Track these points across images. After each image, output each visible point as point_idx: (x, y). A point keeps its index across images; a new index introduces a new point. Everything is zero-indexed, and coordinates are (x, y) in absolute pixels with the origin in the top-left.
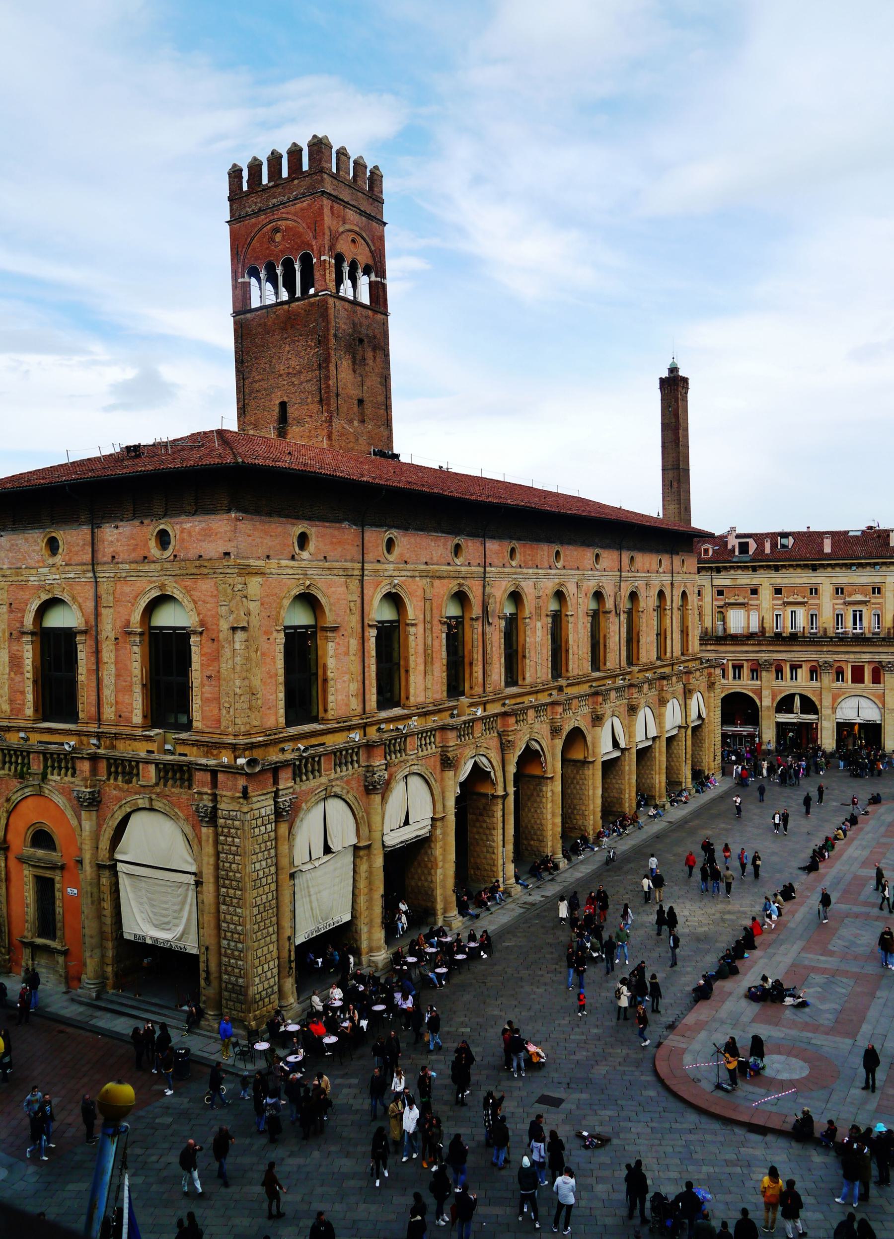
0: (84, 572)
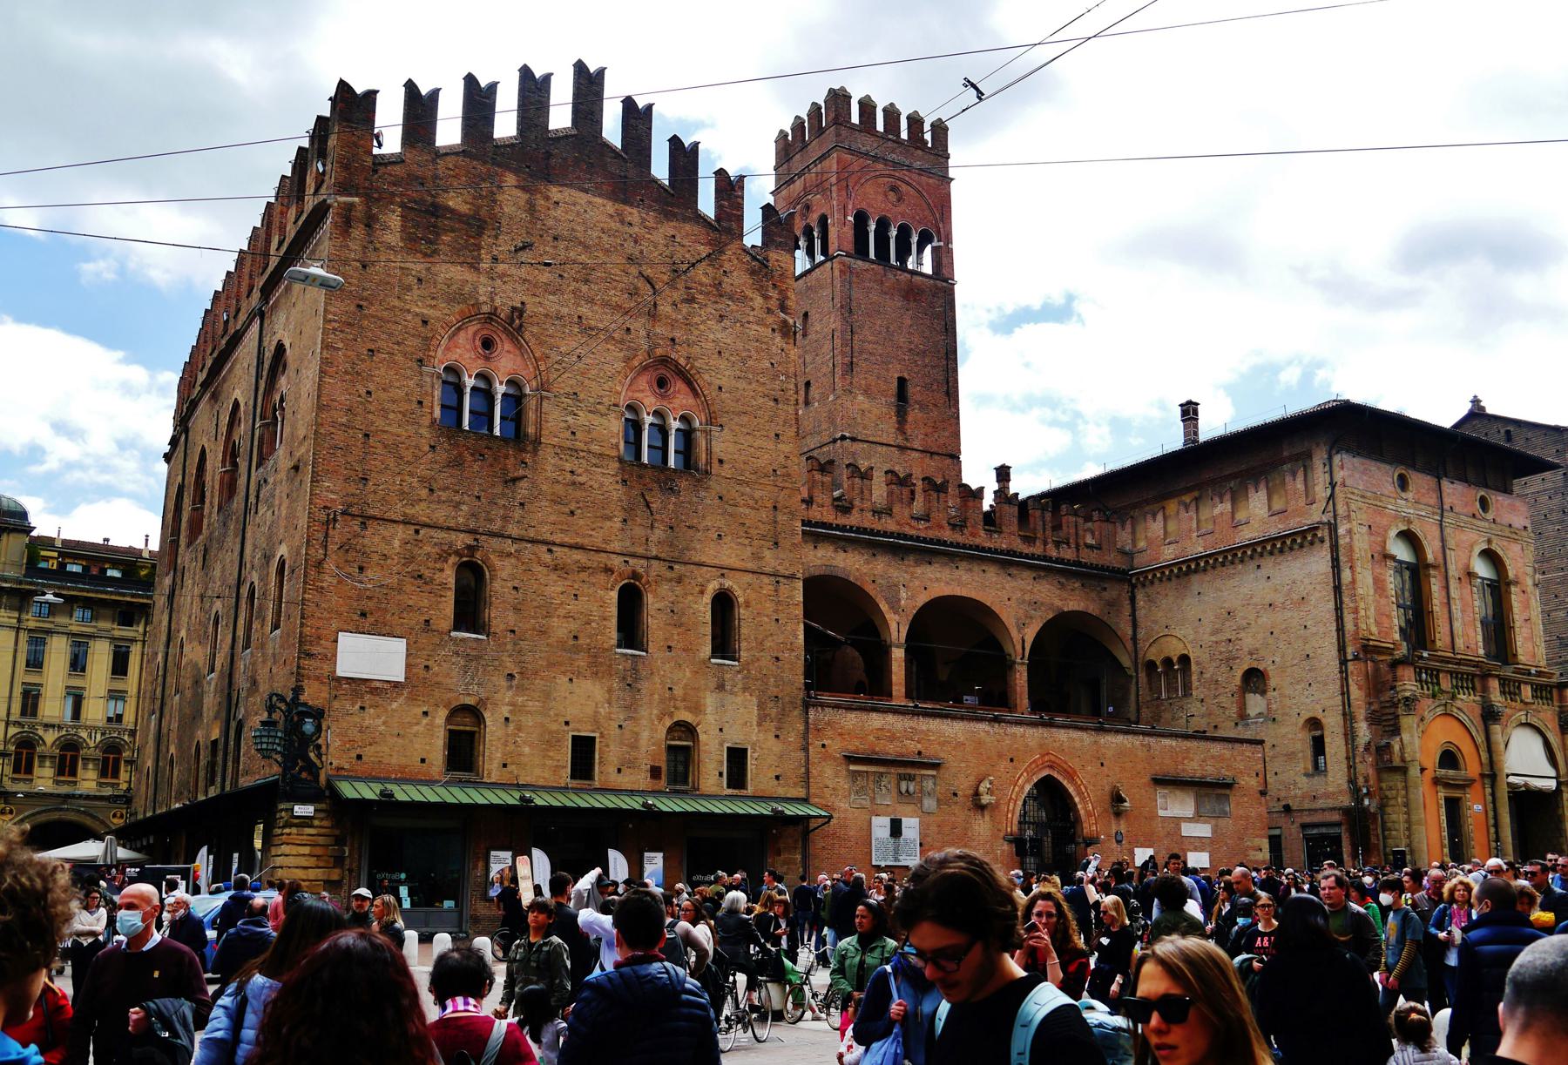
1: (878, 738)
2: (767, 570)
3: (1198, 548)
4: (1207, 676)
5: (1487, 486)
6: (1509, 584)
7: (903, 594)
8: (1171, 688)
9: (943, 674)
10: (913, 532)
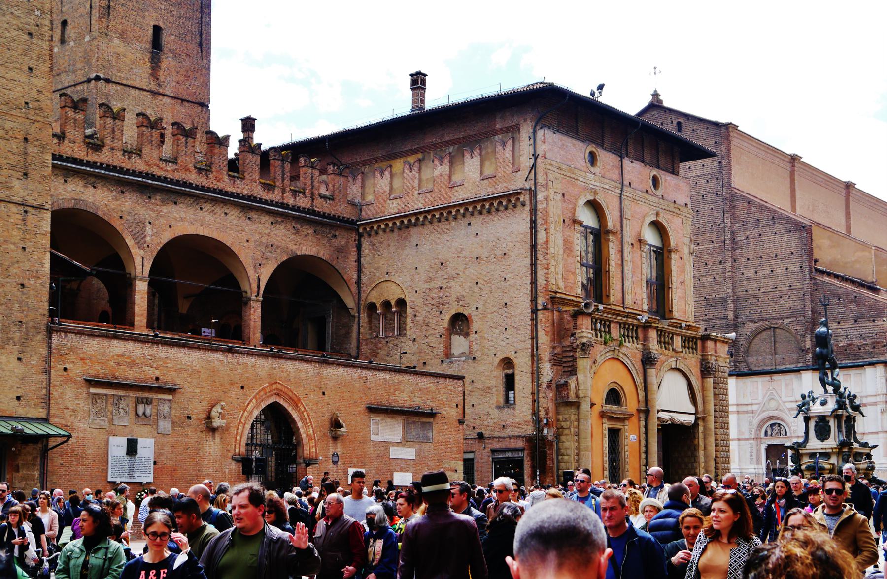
0: (615, 187)
1: (118, 364)
2: (16, 199)
3: (418, 204)
4: (420, 318)
5: (658, 167)
6: (670, 251)
7: (149, 231)
8: (388, 328)
9: (184, 307)
10: (161, 174)
